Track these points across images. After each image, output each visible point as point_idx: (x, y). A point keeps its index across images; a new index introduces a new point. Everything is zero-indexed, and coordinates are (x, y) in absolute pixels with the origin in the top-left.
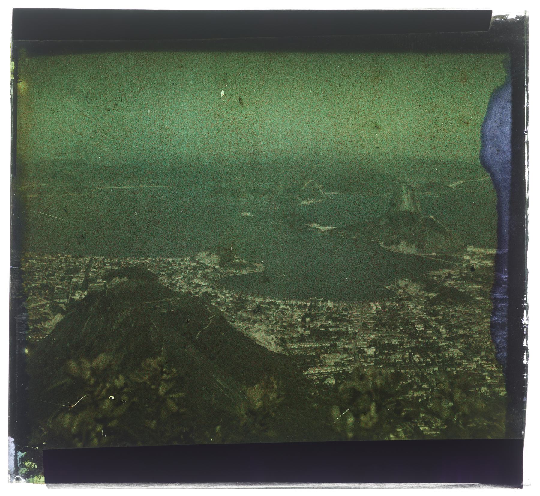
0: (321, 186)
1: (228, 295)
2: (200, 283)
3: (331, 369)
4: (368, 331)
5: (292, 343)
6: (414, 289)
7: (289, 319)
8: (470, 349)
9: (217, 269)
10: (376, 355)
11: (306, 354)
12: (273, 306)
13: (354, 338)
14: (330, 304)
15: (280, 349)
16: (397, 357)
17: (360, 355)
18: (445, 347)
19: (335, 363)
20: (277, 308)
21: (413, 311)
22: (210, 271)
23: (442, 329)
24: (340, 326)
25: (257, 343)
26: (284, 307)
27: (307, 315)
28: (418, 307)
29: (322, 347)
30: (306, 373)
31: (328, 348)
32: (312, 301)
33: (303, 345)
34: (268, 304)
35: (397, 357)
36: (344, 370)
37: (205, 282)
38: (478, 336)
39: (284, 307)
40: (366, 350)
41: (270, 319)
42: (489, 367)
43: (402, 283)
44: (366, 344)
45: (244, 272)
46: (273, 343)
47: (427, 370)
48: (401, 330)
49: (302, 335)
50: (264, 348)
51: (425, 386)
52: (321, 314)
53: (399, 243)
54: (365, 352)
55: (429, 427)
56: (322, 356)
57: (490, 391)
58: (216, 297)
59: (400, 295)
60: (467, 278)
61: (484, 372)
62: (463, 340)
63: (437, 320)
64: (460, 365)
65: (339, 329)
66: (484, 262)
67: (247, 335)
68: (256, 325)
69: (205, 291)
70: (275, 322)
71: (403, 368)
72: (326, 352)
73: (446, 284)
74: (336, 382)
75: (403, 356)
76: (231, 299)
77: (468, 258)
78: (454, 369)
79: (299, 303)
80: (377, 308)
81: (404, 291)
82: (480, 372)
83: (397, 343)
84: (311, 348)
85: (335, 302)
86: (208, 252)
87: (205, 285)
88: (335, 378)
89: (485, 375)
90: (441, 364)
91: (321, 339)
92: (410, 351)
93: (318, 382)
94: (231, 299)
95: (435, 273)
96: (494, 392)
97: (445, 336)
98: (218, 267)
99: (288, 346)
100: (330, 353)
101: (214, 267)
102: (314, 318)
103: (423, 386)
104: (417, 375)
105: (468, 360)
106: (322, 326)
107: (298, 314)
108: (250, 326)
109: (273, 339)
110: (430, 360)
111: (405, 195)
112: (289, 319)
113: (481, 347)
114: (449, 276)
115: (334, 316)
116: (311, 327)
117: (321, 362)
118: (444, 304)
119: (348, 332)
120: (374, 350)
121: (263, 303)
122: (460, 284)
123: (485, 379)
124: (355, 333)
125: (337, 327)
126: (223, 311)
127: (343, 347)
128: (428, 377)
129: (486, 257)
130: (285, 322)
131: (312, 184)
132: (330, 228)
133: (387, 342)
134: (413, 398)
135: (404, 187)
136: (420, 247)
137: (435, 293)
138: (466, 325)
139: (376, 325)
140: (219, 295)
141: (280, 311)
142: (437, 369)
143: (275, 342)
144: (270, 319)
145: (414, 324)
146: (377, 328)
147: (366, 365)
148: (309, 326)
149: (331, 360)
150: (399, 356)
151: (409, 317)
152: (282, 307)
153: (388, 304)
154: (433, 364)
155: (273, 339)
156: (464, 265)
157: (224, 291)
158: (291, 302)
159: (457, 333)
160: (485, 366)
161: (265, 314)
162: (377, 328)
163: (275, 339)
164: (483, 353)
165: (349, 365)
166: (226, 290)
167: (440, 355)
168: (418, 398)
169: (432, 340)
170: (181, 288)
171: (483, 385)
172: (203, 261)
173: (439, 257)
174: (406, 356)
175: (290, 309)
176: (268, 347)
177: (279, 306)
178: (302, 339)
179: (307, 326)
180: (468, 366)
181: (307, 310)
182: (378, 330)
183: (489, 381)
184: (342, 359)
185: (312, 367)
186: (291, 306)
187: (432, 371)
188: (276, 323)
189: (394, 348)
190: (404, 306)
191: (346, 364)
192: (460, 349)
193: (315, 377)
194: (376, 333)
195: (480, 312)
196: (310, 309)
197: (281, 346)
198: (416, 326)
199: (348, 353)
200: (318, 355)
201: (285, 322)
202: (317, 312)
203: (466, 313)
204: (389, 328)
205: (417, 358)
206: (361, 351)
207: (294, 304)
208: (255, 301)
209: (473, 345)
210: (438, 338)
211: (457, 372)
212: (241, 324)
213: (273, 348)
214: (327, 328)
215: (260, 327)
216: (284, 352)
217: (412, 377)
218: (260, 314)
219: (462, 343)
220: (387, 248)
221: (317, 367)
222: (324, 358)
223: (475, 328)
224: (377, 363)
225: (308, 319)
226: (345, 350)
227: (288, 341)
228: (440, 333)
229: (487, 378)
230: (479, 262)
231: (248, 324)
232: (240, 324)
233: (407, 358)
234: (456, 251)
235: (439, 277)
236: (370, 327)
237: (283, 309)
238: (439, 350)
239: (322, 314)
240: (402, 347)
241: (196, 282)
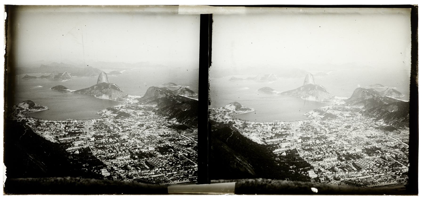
0: (70, 74)
1: (32, 120)
3: (77, 147)
4: (91, 131)
5: (61, 138)
6: (109, 113)
7: (59, 128)
8: (131, 135)
9: (28, 110)
10: (95, 141)
11: (67, 142)
12: (52, 123)
13: (86, 134)
14: (76, 121)
15: (56, 141)
16: (103, 140)
17: (89, 141)
18: (121, 135)
19: (79, 145)
20: (54, 124)
21: (108, 122)
22: (25, 111)
23: (120, 128)
24: (80, 130)
25: (46, 139)
26: (57, 124)
27: (66, 126)
28: (110, 120)
29: (73, 139)
30: (67, 150)
31: (76, 139)
32: (68, 120)
33: (65, 138)
34: (50, 123)
35: (103, 140)
36: (82, 147)
37: (23, 115)
38: (134, 130)
39: (57, 124)
40: (91, 139)
41: (51, 129)
42: (138, 141)
43: (104, 111)
44: (91, 136)
45: (39, 110)
46: (53, 138)
47: (115, 145)
48: (104, 130)
49: (65, 135)
50: (49, 141)
51: (115, 151)
52: (72, 125)
53: (102, 95)
54: (90, 139)
55: (117, 167)
56: (73, 142)
57: (139, 151)
58: (28, 121)
59: (104, 116)
60: (128, 108)
61: (136, 143)
62: (128, 132)
63: (118, 125)
64: (127, 141)
65: (79, 131)
66: (134, 101)
67: (42, 136)
68: (45, 132)
69: (23, 119)
71: (106, 144)
72: (75, 141)
73: (121, 111)
74: (79, 152)
75: (105, 140)
76: (34, 122)
77: (129, 100)
78: (125, 143)
79: (63, 122)
80: (95, 122)
81: (105, 114)
82: (135, 144)
83: (103, 135)
84: (68, 139)
85: (77, 120)
87: (23, 117)
89: (137, 145)
90: (120, 142)
91: (73, 136)
92: (108, 138)
93: (72, 153)
94: (34, 122)
95: (116, 106)
96: (140, 151)
97: (121, 131)
98: (28, 109)
99: (59, 139)
100: (76, 141)
102: (69, 127)
103: (114, 151)
104: (111, 147)
105: (130, 139)
106: (73, 130)
107: (63, 126)
108: (43, 132)
109: (53, 137)
110: (116, 140)
111: (103, 77)
112: (59, 128)
113: (135, 134)
114: (122, 107)
115: (78, 126)
116: (68, 131)
117: (73, 145)
118: (120, 118)
119: (83, 132)
120: (94, 138)
121: (48, 123)
122: (126, 110)
123: (137, 146)
124: (86, 132)
125: (79, 130)
126: (31, 127)
127: (81, 138)
128: (116, 147)
129: (135, 99)
130: (57, 130)
131: (66, 73)
132: (74, 91)
133: (99, 135)
134: (110, 156)
135: (103, 74)
136: (110, 96)
137: (117, 114)
138: (129, 126)
139: (94, 128)
140: (29, 120)
142: (118, 144)
143: (54, 138)
144: (51, 129)
145: (109, 127)
146: (95, 130)
147: (91, 145)
148: (68, 131)
149: (77, 143)
150: (104, 140)
151: (107, 124)
152: (56, 124)
153: (99, 120)
154: (117, 142)
155: (53, 137)
156: (127, 103)
158: (60, 121)
159: (126, 129)
160: (136, 141)
161: (49, 127)
162: (95, 130)
163: (54, 137)
164: (136, 136)
165: (84, 145)
166: (32, 118)
167: (120, 138)
168: (112, 156)
169: (116, 133)
171: (136, 149)
172: (22, 107)
174: (106, 140)
175: (59, 124)
176: (50, 141)
177: (55, 123)
178: (65, 136)
179: (67, 131)
181: (66, 124)
182: (95, 130)
184: (81, 143)
185: (69, 147)
186: (60, 123)
187: (117, 145)
188: (54, 131)
189: (102, 137)
190: (105, 120)
191: (83, 145)
192: (127, 135)
193: (71, 151)
194: (95, 131)
195: (134, 120)
196: (67, 124)
197: (56, 140)
198: (110, 128)
199: (84, 140)
200: (71, 142)
201: (57, 130)
202: (71, 125)
203: (129, 121)
204: (100, 129)
205: (111, 140)
206: (89, 139)
207: (61, 122)
208: (44, 122)
209: (132, 133)
210: (119, 132)
211: (127, 144)
212: (39, 132)
213: (53, 141)
214: (75, 131)
215: (47, 133)
216: (57, 142)
217: (109, 148)
218: (47, 127)
219: (128, 133)
220: (98, 97)
221: (71, 147)
222: (74, 143)
224: (95, 143)
225: (67, 128)
226: (83, 139)
227: (59, 137)
228: (119, 130)
229: (137, 146)
230: (133, 101)
231: (42, 131)
232: (38, 132)
233: (107, 141)
234: (124, 97)
235: (118, 108)
236: (92, 129)
237: (56, 124)
238: (119, 136)
239: (73, 125)
240: (105, 136)
241: (19, 116)
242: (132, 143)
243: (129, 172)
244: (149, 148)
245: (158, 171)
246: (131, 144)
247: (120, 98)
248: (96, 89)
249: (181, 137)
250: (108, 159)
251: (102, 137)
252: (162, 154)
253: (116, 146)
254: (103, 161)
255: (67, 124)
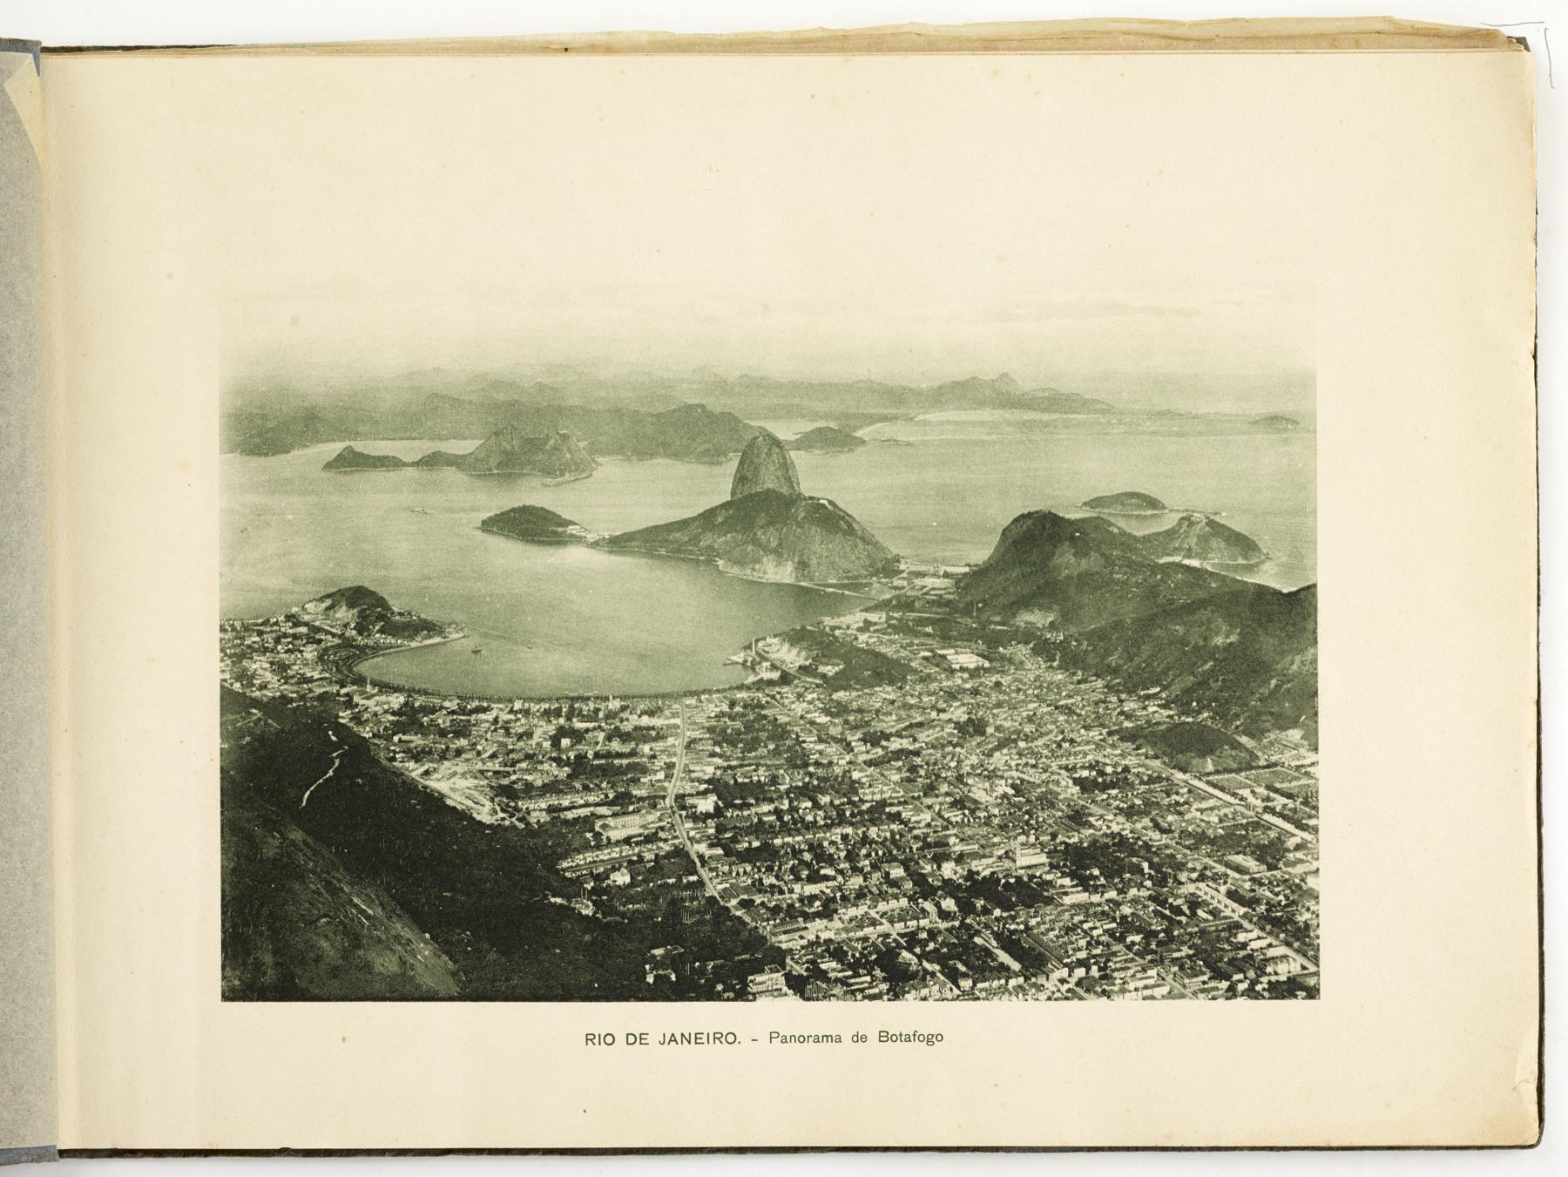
2: (309, 675)
61: (946, 828)
70: (487, 754)
86: (328, 602)
88: (630, 871)
101: (343, 634)
123: (947, 844)
141: (502, 728)
144: (479, 748)
157: (369, 688)
170: (263, 687)
173: (843, 586)
180: (913, 819)
183: (958, 848)
196: (569, 719)
223: (924, 736)
224: (720, 829)
232: (407, 764)
242: (923, 824)
243: (909, 992)
244: (1018, 852)
245: (1070, 986)
246: (916, 832)
247: (856, 578)
248: (727, 527)
249: (1190, 791)
250: (792, 915)
251: (759, 792)
252: (1086, 890)
253: (832, 843)
254: (765, 928)
255: (569, 719)
